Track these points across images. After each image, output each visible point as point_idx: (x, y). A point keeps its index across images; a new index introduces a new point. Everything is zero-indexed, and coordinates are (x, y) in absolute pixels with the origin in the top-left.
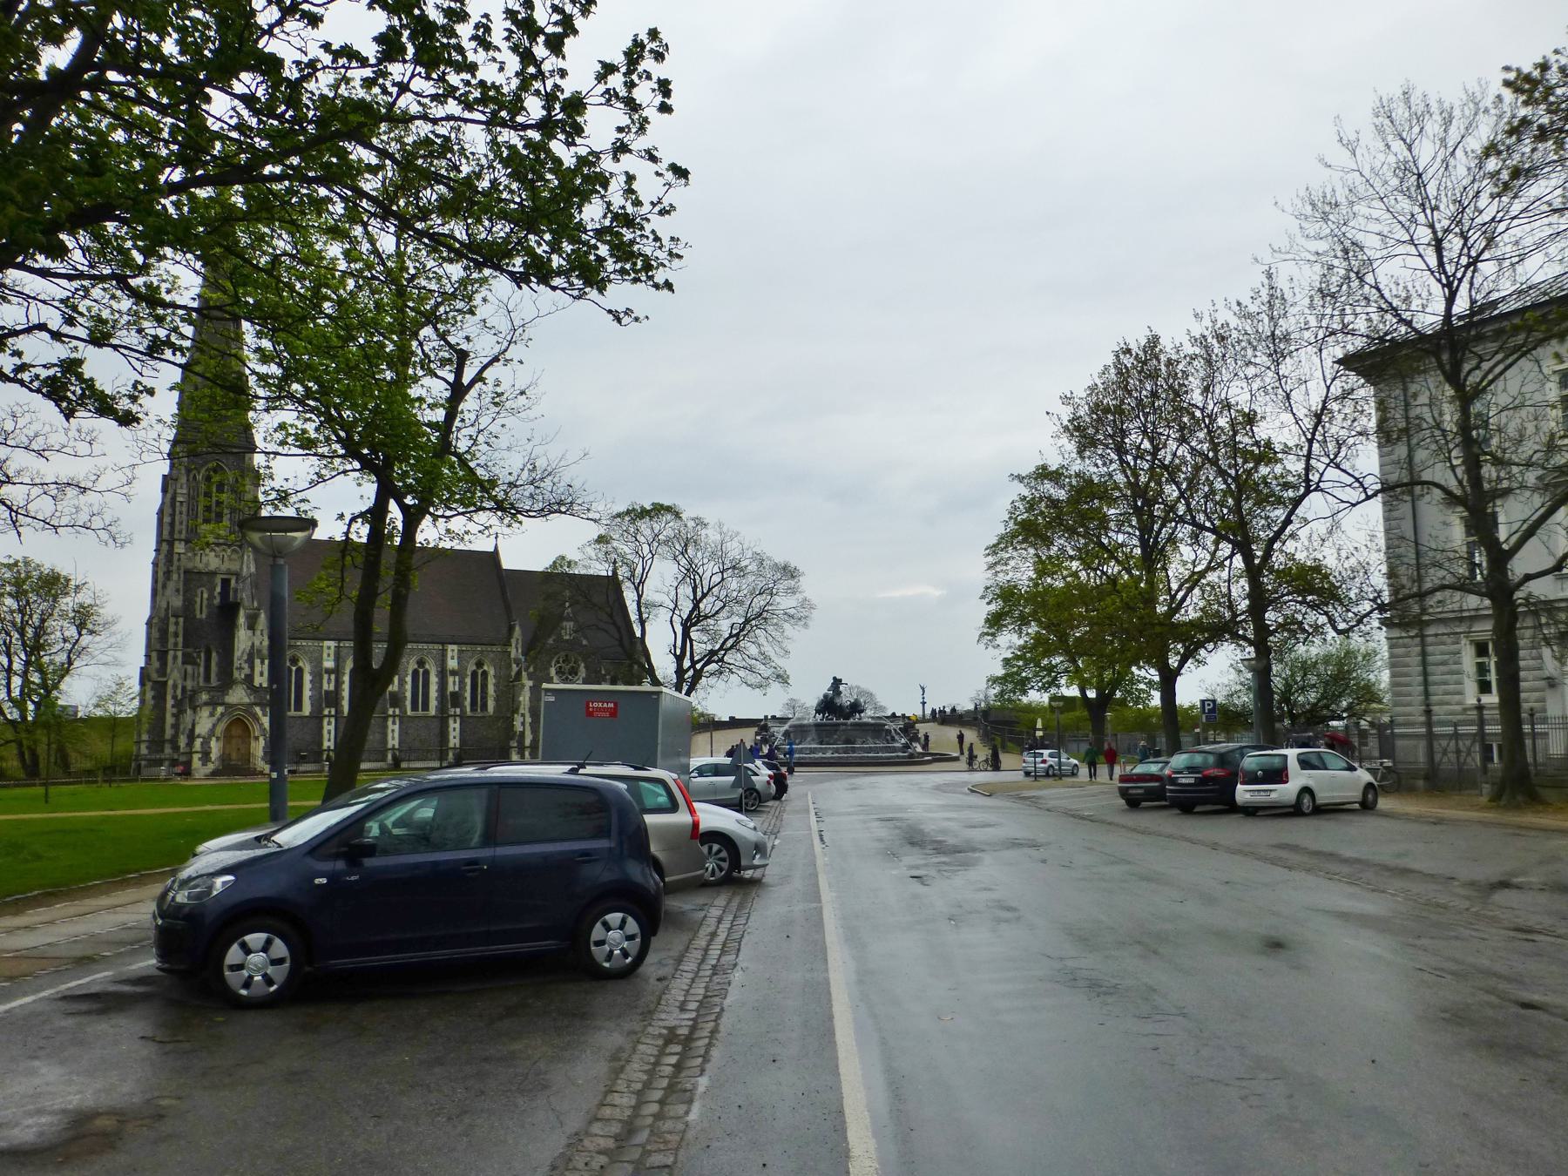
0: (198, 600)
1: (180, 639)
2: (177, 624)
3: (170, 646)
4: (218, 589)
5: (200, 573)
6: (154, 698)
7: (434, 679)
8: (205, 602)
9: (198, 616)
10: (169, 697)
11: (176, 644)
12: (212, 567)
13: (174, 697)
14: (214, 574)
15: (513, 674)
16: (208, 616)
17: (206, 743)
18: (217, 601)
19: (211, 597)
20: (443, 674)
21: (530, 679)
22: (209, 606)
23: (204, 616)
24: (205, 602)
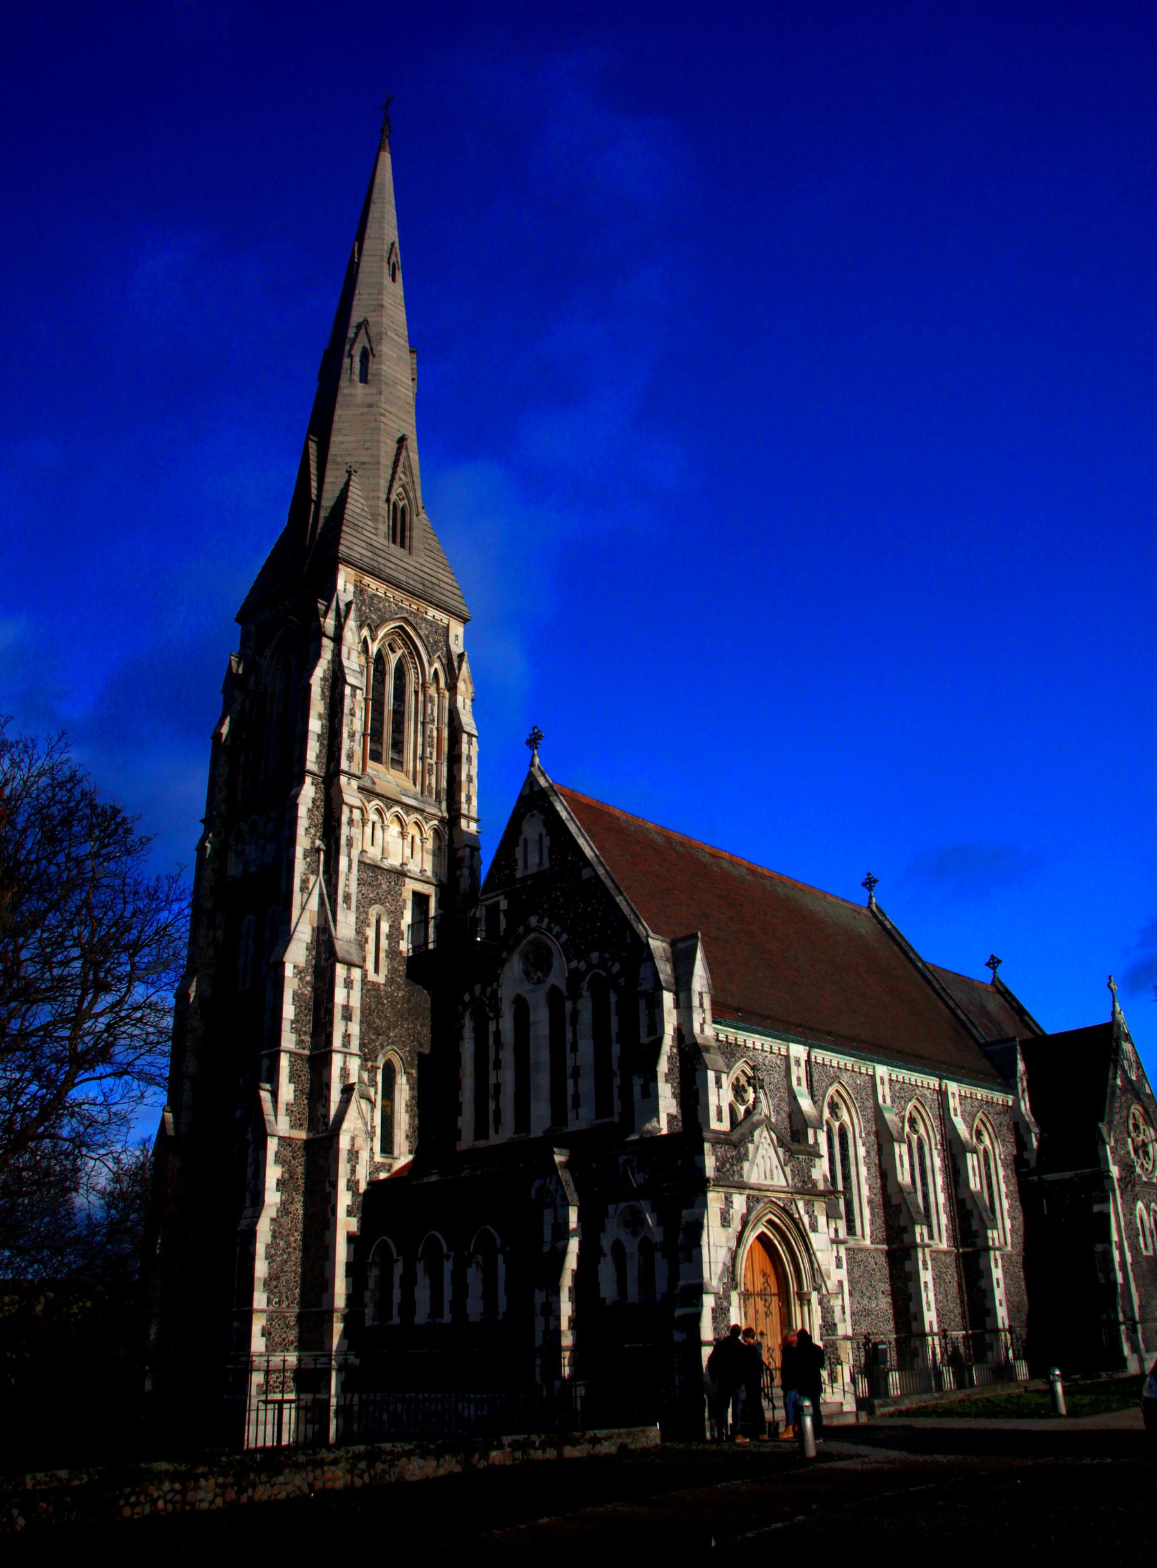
0: (371, 933)
1: (355, 1028)
2: (348, 984)
3: (337, 1042)
4: (407, 918)
5: (374, 868)
6: (281, 1184)
7: (937, 1162)
8: (384, 943)
9: (372, 976)
10: (342, 1184)
11: (347, 1037)
12: (394, 861)
13: (352, 1185)
14: (400, 874)
15: (1031, 1157)
16: (390, 981)
17: (721, 1312)
18: (404, 946)
19: (395, 935)
20: (954, 1150)
21: (1114, 1164)
22: (393, 952)
23: (381, 979)
24: (384, 943)
